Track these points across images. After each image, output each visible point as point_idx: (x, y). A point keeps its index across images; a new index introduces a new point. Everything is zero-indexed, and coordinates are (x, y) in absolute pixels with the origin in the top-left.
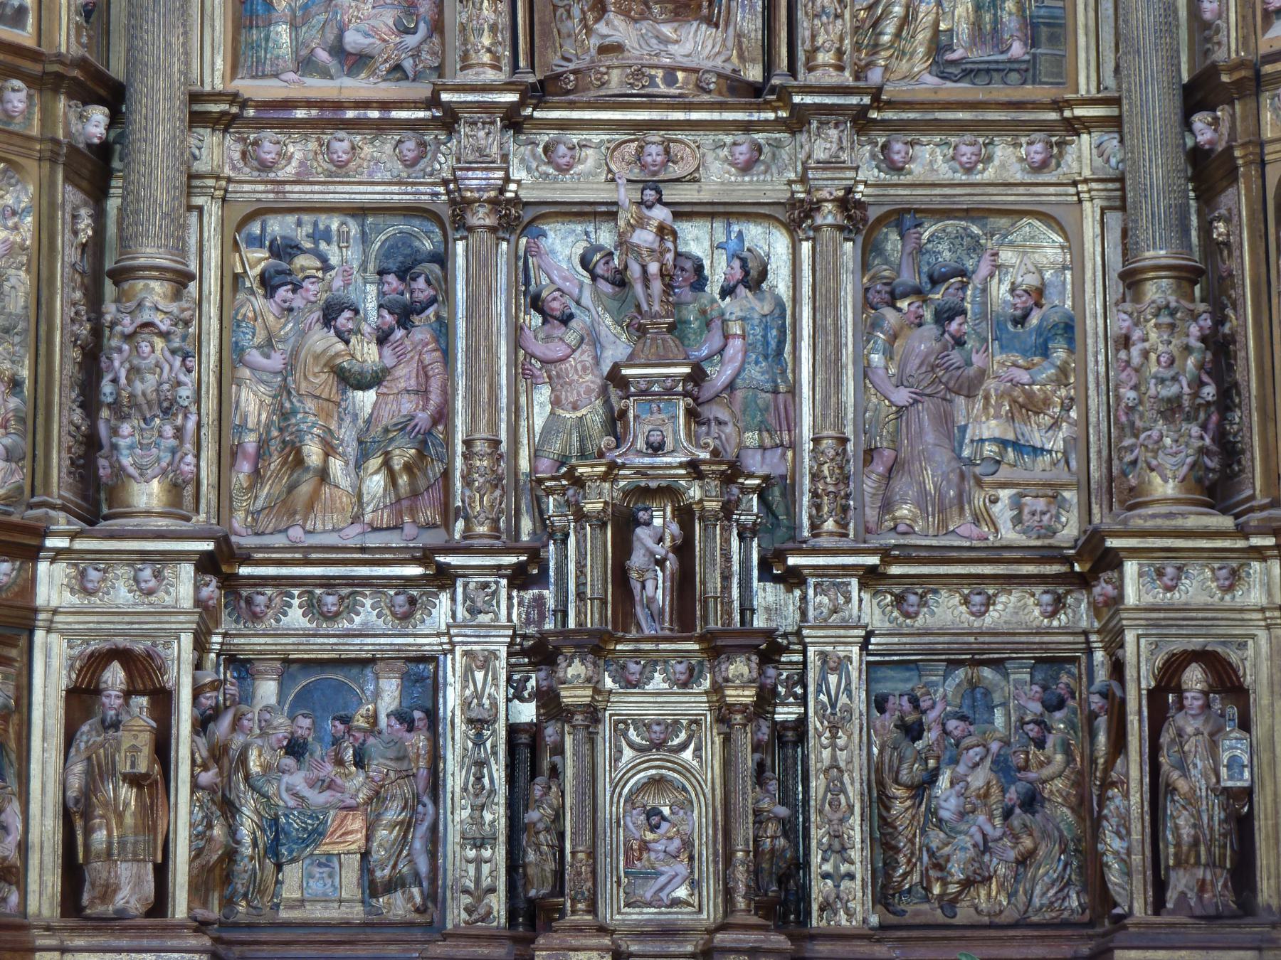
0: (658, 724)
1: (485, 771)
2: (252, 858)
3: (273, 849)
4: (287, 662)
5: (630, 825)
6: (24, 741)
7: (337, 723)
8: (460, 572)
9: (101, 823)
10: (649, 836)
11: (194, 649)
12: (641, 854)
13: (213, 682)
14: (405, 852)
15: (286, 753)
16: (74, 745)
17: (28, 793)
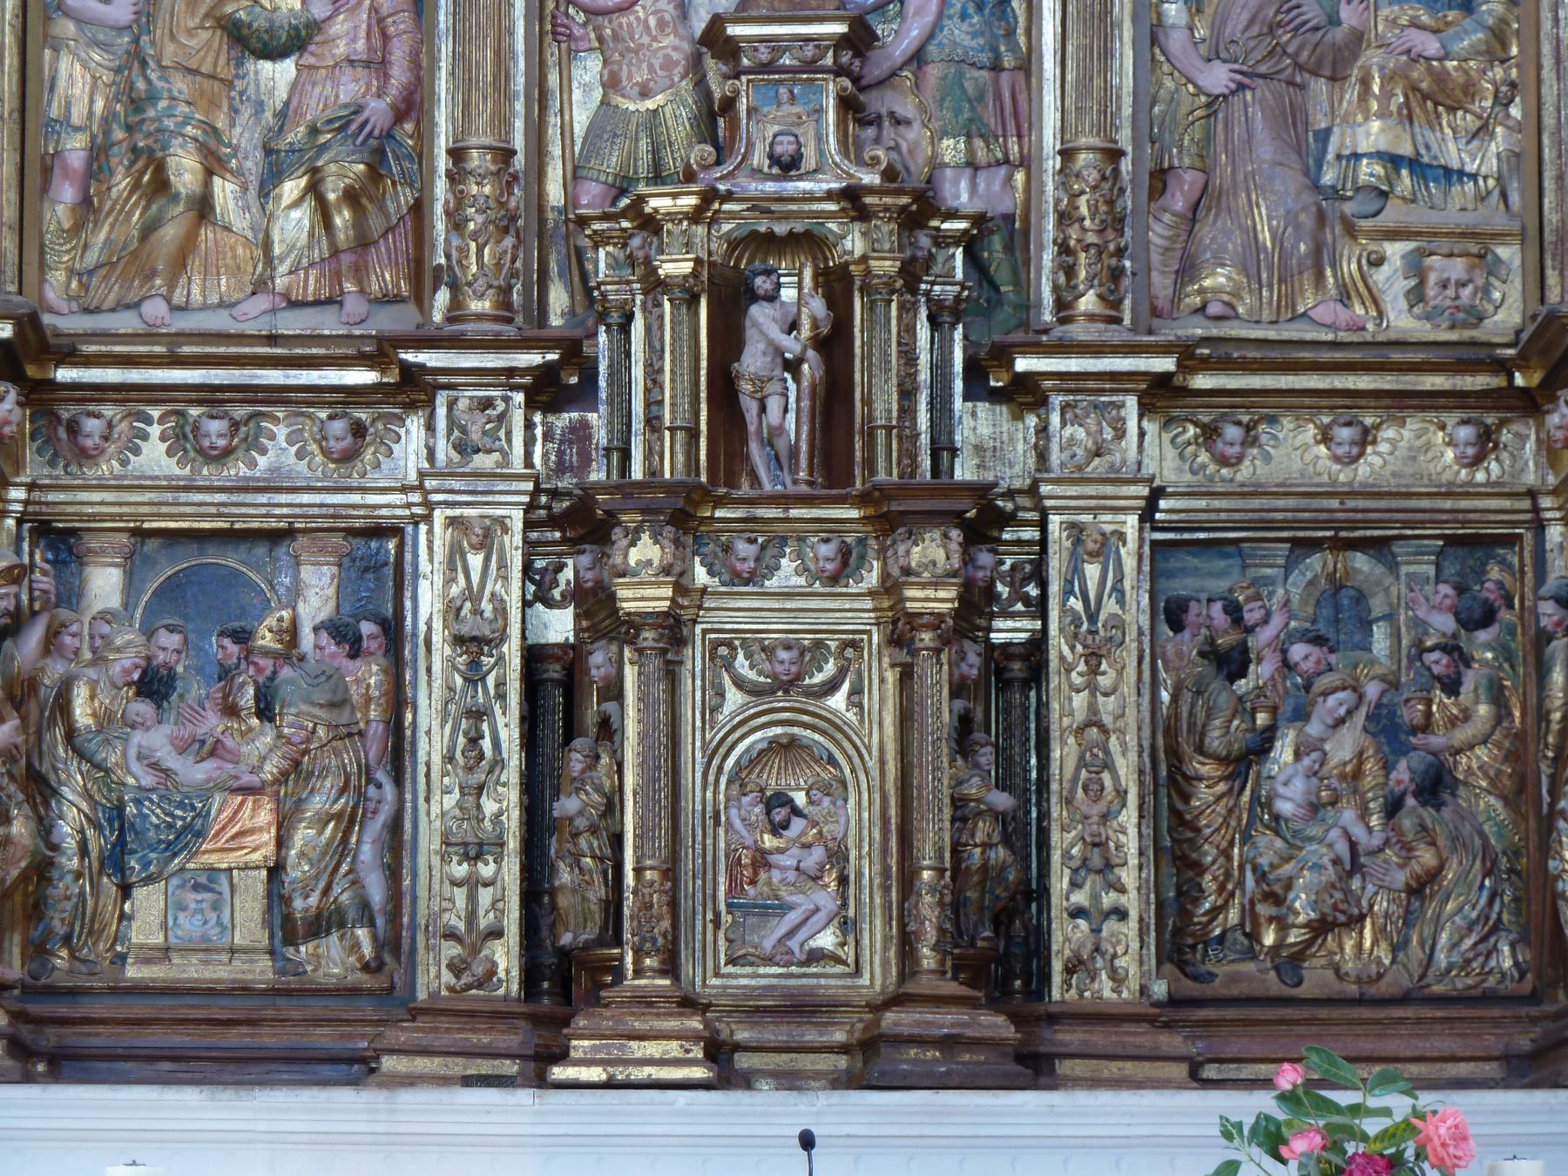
0: (788, 647)
1: (485, 726)
2: (78, 875)
3: (115, 860)
4: (140, 534)
5: (738, 823)
7: (227, 642)
8: (443, 379)
10: (769, 841)
12: (756, 873)
13: (10, 569)
14: (344, 868)
15: (138, 694)
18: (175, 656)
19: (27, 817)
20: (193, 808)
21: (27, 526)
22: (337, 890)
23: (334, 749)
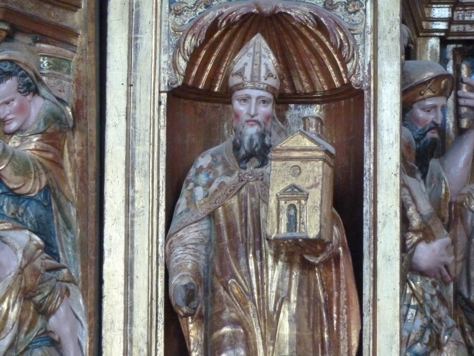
6: (92, 184)
9: (234, 336)
11: (403, 21)
13: (438, 78)
16: (185, 192)
17: (100, 282)
19: (458, 343)
21: (450, 47)
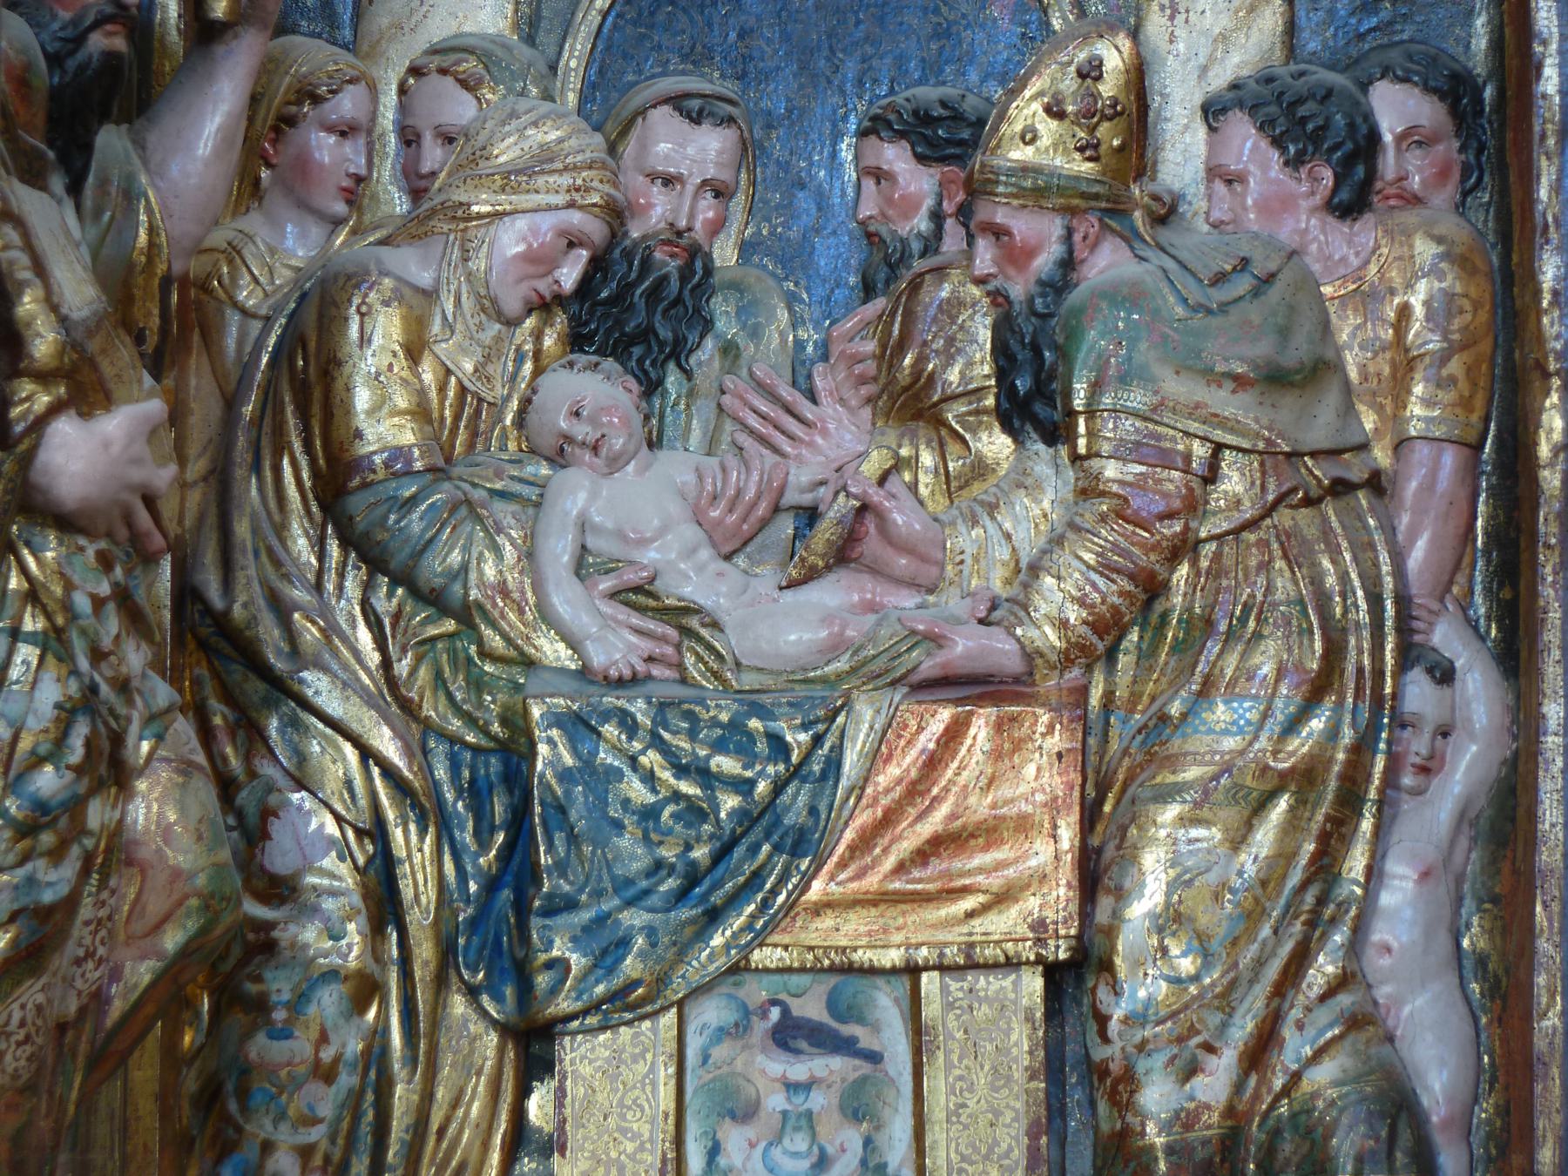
2: (365, 989)
7: (895, 156)
14: (1324, 967)
15: (576, 341)
18: (707, 209)
20: (779, 747)
22: (1294, 1046)
23: (1286, 538)
